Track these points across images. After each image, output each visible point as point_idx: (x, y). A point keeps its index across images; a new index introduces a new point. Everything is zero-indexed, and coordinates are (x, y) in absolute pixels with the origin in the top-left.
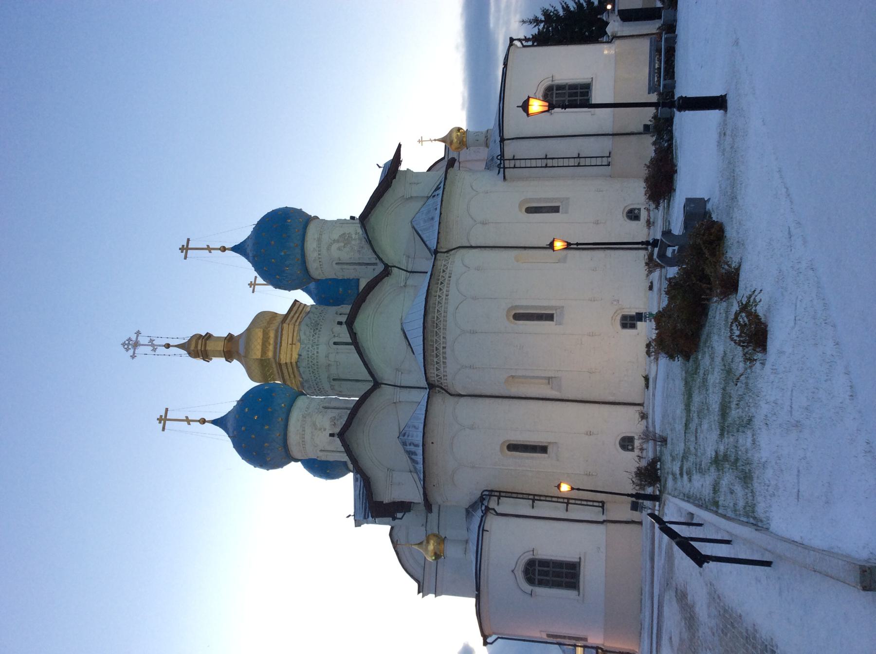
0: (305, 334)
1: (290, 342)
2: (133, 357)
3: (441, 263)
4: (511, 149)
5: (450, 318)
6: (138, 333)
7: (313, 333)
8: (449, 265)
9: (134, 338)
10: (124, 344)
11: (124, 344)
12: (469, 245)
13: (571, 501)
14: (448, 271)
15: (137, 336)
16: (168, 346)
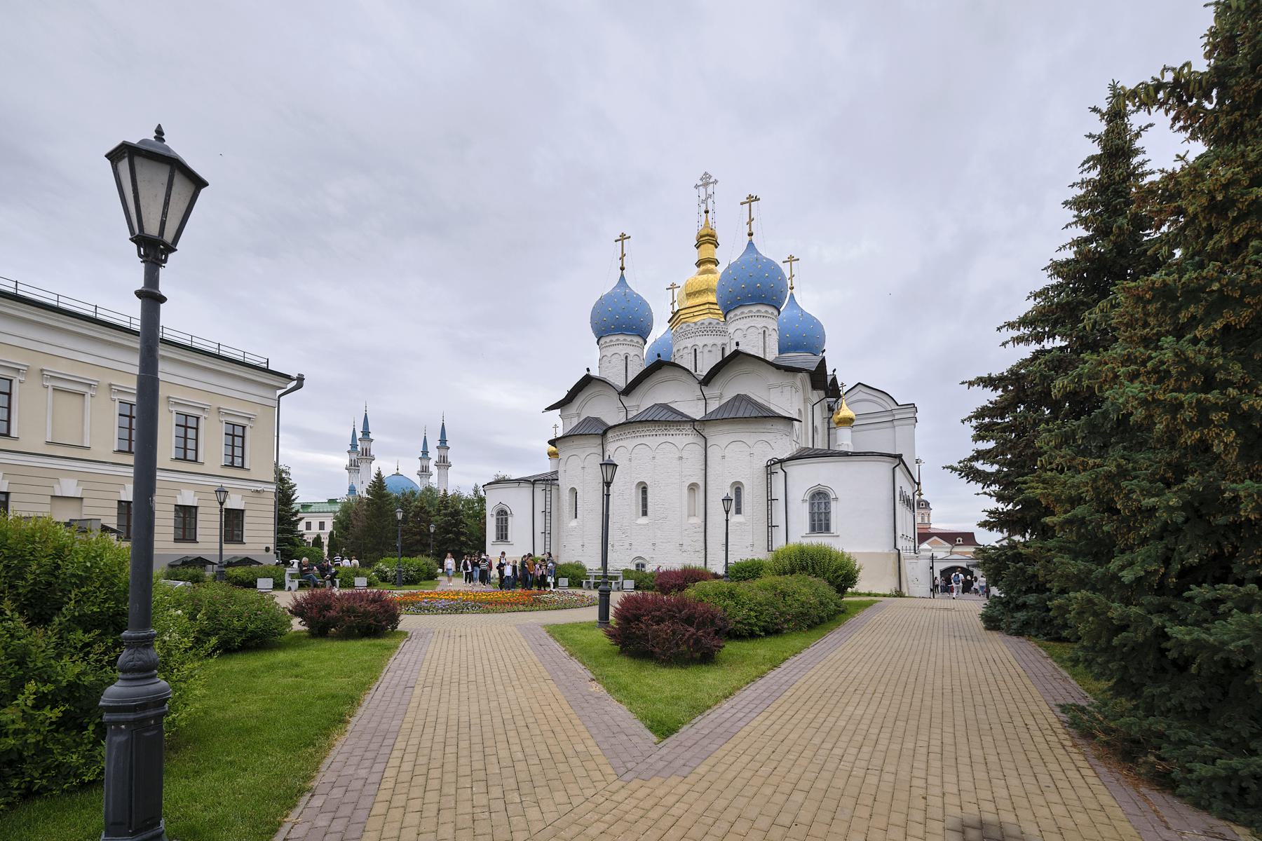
0: (703, 324)
1: (695, 314)
2: (697, 187)
3: (688, 427)
4: (777, 467)
5: (639, 441)
6: (716, 182)
7: (703, 329)
8: (684, 432)
9: (711, 181)
10: (706, 174)
11: (706, 174)
12: (708, 446)
13: (547, 536)
14: (678, 432)
15: (713, 183)
16: (707, 212)
